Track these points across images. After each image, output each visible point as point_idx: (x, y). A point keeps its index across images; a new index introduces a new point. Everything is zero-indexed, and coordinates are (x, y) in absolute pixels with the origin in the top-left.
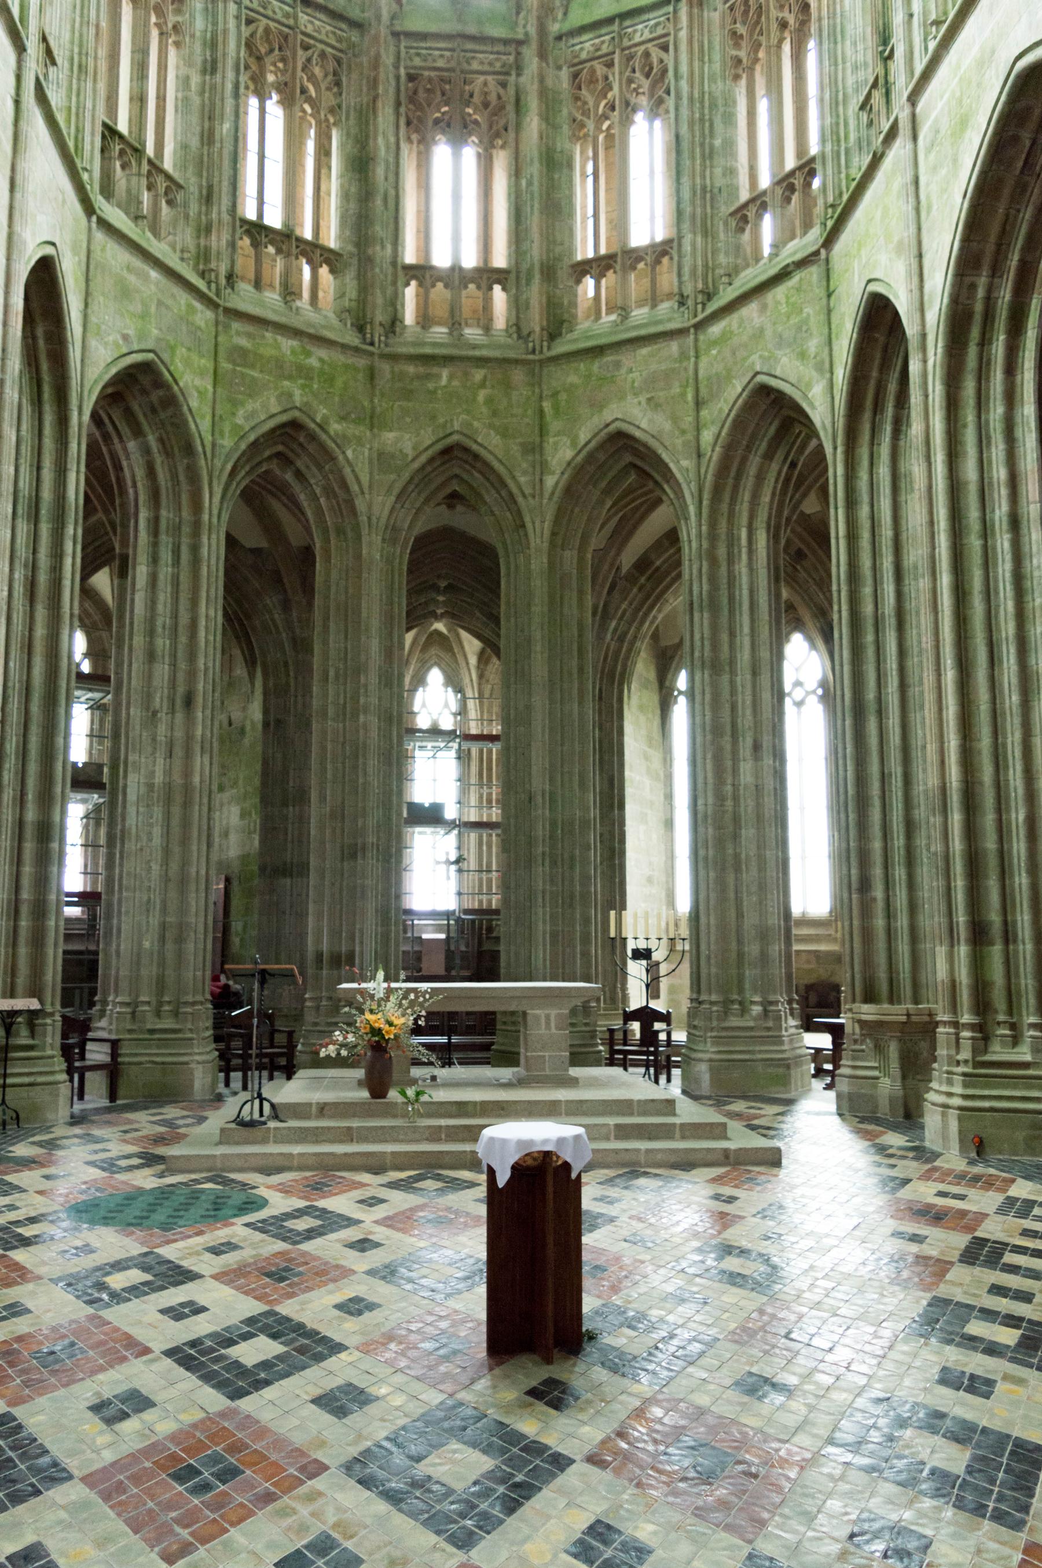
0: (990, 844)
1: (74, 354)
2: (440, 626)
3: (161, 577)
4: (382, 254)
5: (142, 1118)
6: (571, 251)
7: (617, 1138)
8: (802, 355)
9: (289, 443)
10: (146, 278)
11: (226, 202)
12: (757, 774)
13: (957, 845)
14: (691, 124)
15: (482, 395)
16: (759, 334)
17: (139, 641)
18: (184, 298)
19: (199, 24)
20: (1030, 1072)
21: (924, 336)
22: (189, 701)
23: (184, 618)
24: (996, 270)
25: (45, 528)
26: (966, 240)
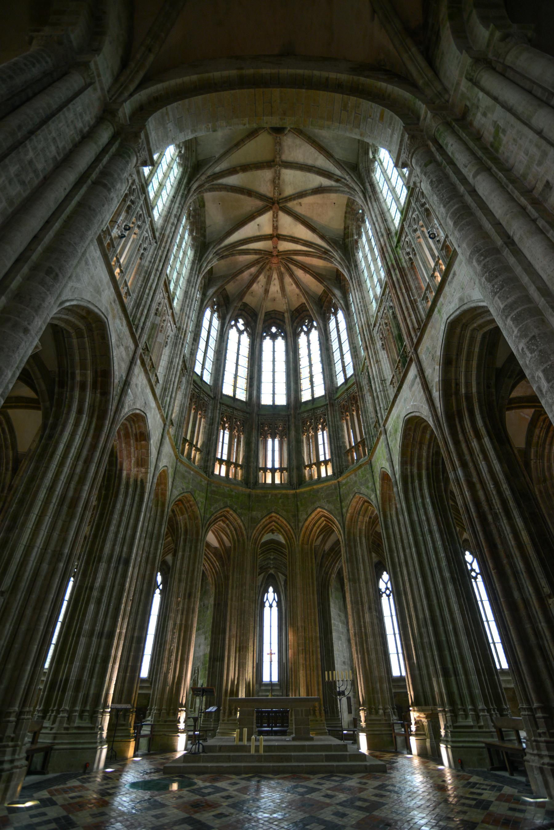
0: (444, 638)
1: (168, 493)
2: (272, 571)
3: (186, 556)
4: (253, 465)
5: (158, 757)
6: (304, 462)
7: (326, 761)
8: (368, 487)
10: (190, 473)
11: (212, 455)
12: (371, 617)
13: (433, 639)
14: (333, 431)
15: (280, 501)
16: (355, 482)
17: (177, 575)
19: (210, 415)
20: (474, 730)
21: (396, 481)
22: (190, 595)
23: (191, 569)
24: (412, 465)
25: (154, 541)
26: (402, 457)
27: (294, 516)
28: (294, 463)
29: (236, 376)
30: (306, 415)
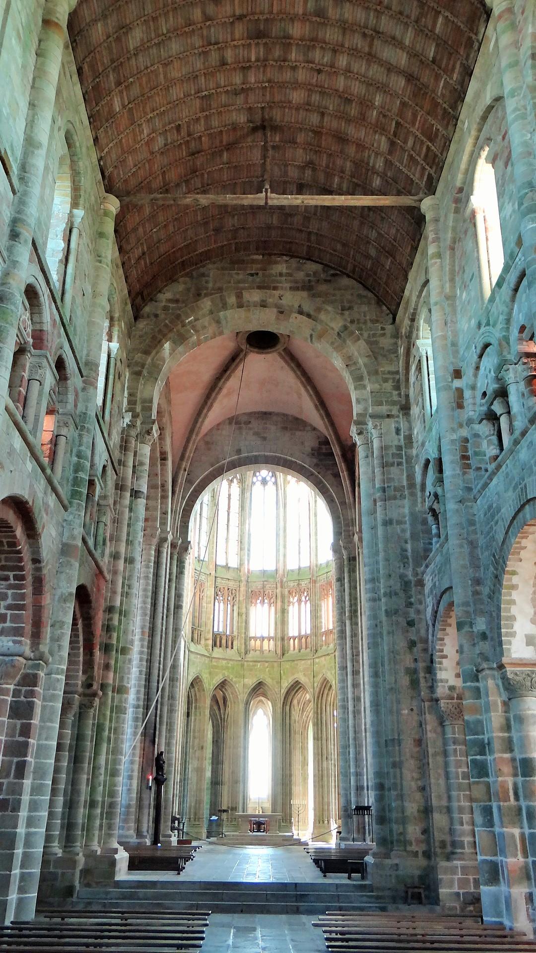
9: (223, 685)
18: (204, 658)
22: (202, 748)
27: (277, 682)
28: (279, 635)
29: (227, 539)
30: (292, 584)
